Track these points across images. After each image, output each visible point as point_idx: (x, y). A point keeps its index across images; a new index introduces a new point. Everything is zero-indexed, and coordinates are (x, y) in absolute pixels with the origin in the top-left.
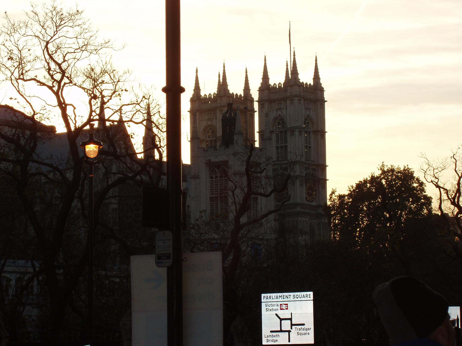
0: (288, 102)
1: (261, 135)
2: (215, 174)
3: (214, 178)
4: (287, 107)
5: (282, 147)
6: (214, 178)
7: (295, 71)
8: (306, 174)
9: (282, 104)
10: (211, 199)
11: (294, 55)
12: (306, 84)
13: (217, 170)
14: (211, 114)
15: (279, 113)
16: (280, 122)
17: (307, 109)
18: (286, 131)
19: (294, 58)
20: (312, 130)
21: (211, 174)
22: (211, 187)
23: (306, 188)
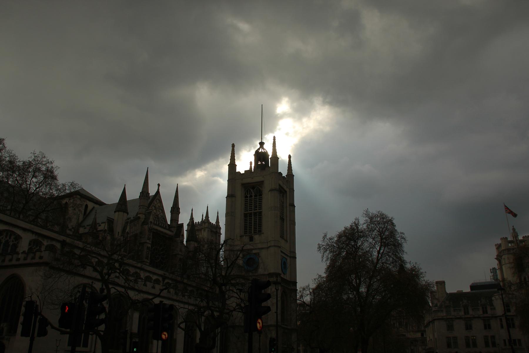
2: (250, 194)
3: (249, 197)
6: (249, 197)
10: (246, 215)
13: (252, 190)
14: (198, 232)
21: (245, 194)
22: (245, 205)
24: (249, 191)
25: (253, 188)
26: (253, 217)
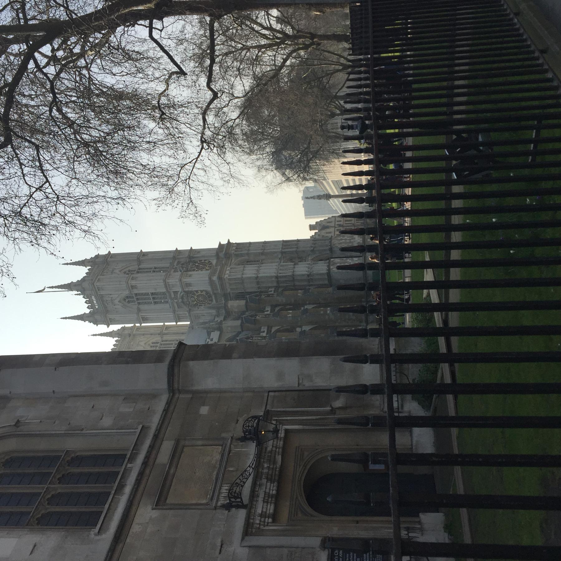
0: (102, 293)
1: (143, 320)
4: (109, 294)
5: (154, 298)
7: (69, 287)
8: (181, 271)
9: (107, 299)
11: (52, 287)
12: (86, 273)
15: (116, 302)
16: (127, 300)
17: (112, 272)
18: (136, 294)
19: (56, 287)
20: (137, 266)
23: (197, 271)
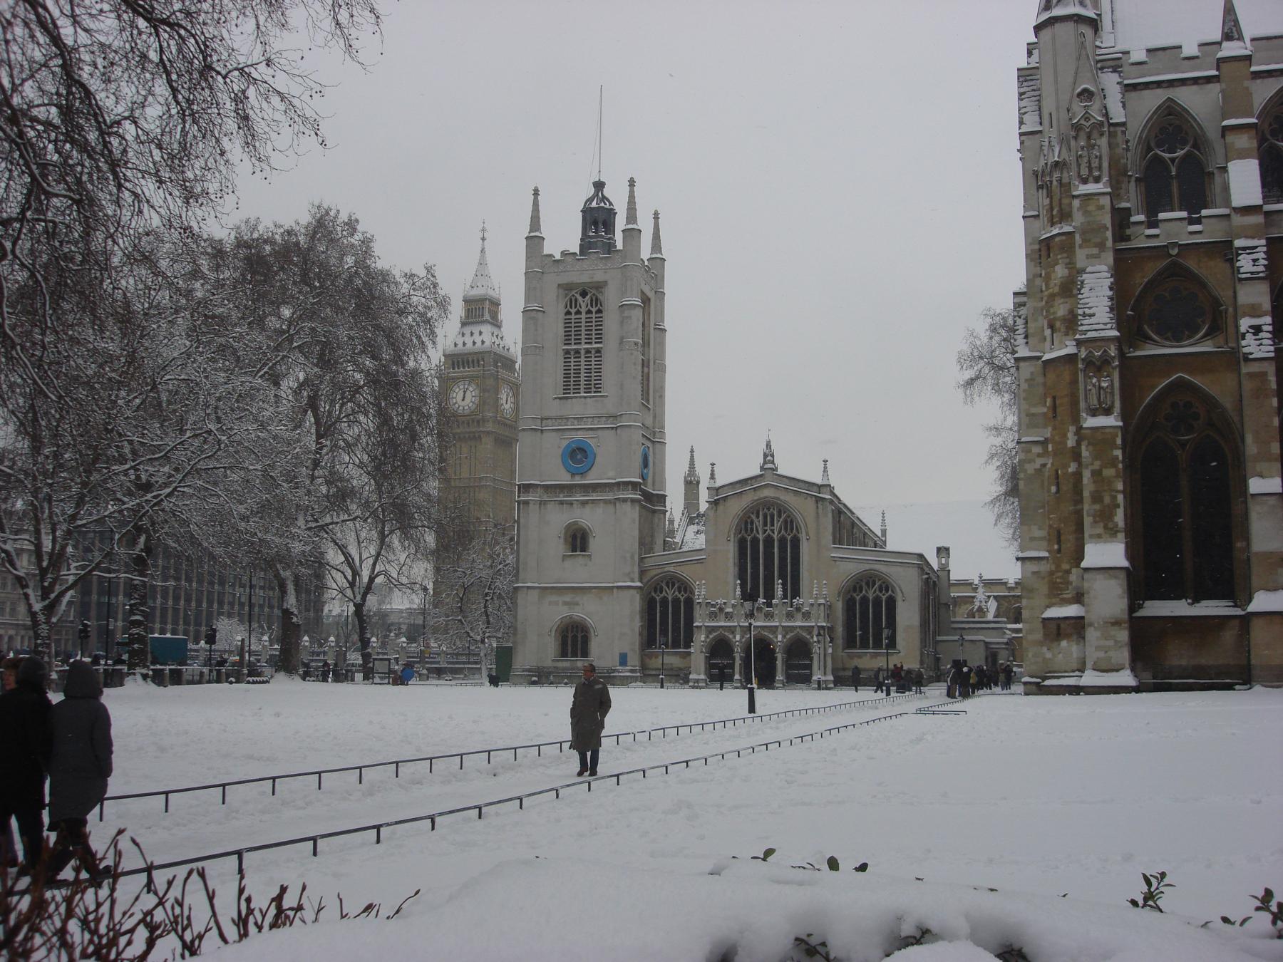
10: (567, 352)
13: (580, 299)
24: (573, 299)
25: (584, 294)
26: (583, 359)
